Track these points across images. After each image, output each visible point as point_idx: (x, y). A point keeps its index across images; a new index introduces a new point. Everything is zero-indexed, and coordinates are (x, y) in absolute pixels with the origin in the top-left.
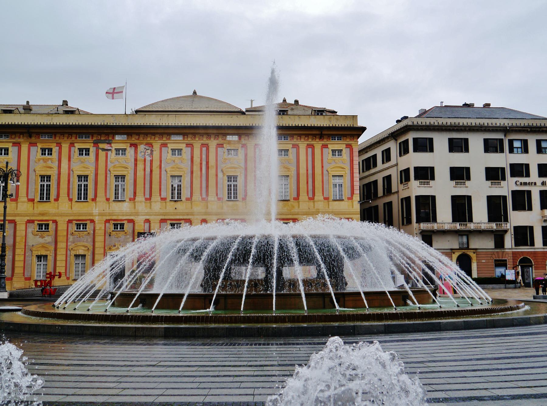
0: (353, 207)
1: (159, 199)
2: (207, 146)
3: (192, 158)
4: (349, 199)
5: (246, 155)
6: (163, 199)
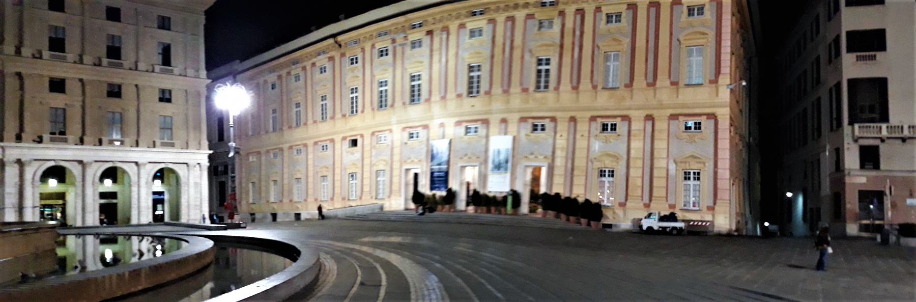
0: (717, 95)
1: (454, 95)
2: (512, 19)
3: (494, 37)
4: (711, 82)
5: (563, 25)
6: (459, 96)
